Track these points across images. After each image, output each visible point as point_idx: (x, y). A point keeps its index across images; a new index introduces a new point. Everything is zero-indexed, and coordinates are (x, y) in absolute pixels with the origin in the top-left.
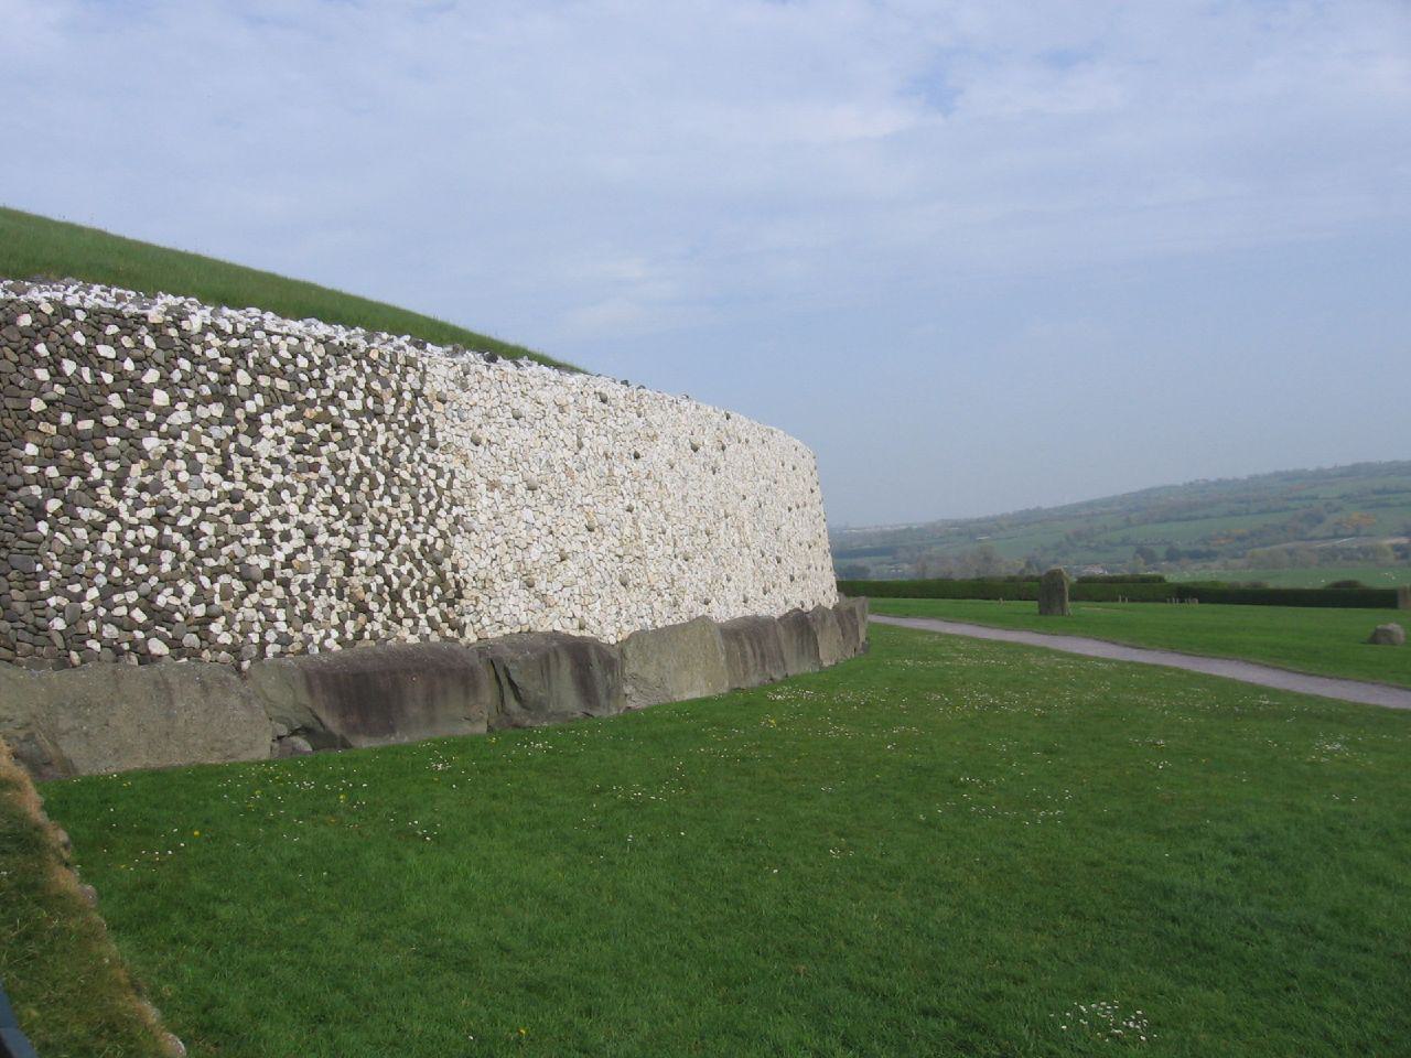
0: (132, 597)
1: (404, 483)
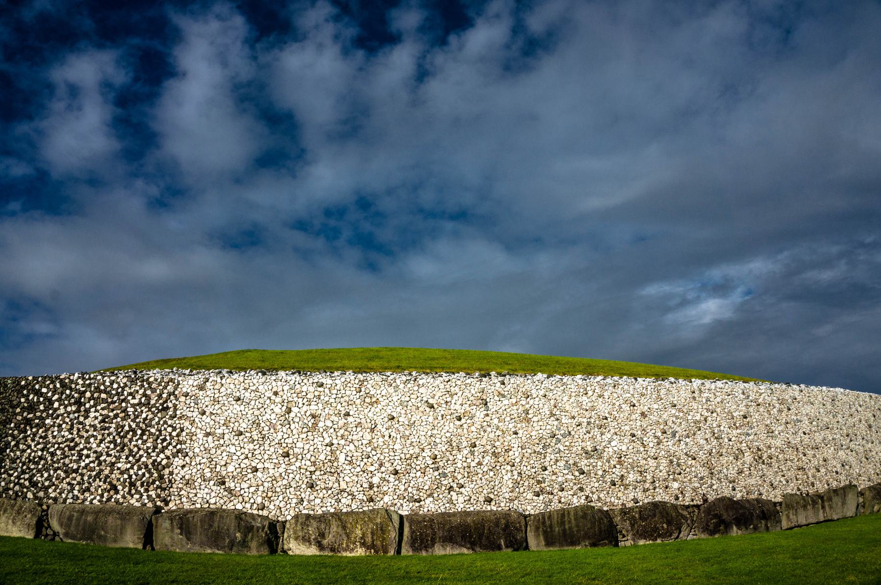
0: (27, 476)
1: (151, 434)
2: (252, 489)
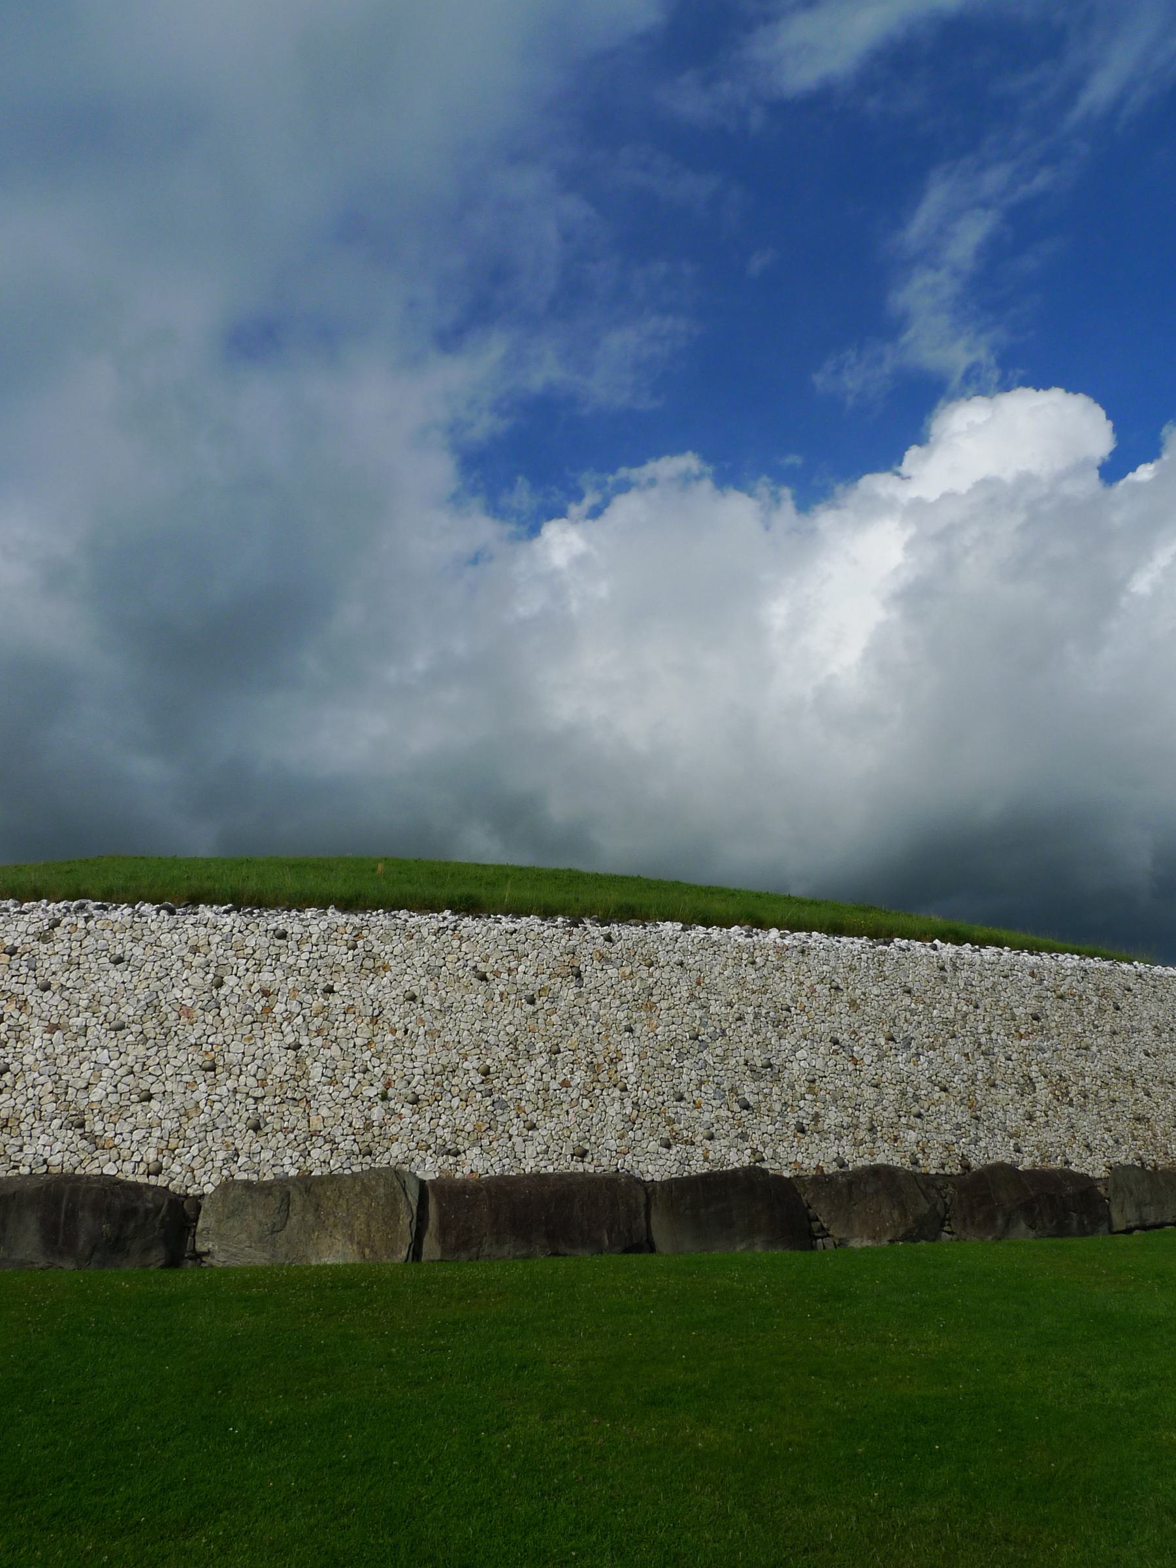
2: (137, 1135)
